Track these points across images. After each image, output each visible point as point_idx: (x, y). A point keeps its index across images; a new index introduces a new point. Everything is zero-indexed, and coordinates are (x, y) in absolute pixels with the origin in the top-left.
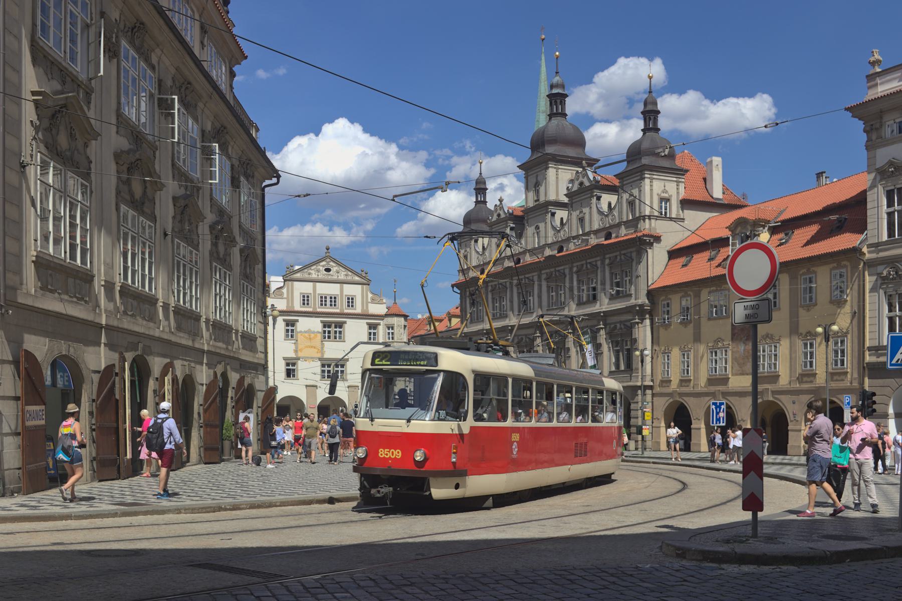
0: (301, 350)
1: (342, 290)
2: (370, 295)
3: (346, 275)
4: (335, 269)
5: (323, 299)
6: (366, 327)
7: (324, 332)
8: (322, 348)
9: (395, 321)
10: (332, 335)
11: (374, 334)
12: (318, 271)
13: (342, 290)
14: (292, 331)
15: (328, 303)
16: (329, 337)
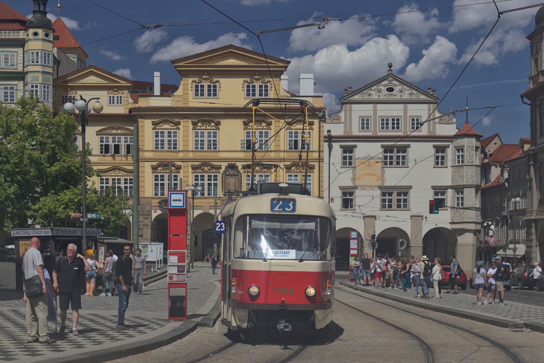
2: (437, 115)
3: (411, 94)
4: (398, 87)
5: (385, 122)
6: (433, 151)
7: (386, 158)
8: (383, 175)
9: (466, 142)
10: (394, 160)
11: (443, 158)
12: (379, 91)
13: (405, 110)
14: (350, 158)
15: (390, 126)
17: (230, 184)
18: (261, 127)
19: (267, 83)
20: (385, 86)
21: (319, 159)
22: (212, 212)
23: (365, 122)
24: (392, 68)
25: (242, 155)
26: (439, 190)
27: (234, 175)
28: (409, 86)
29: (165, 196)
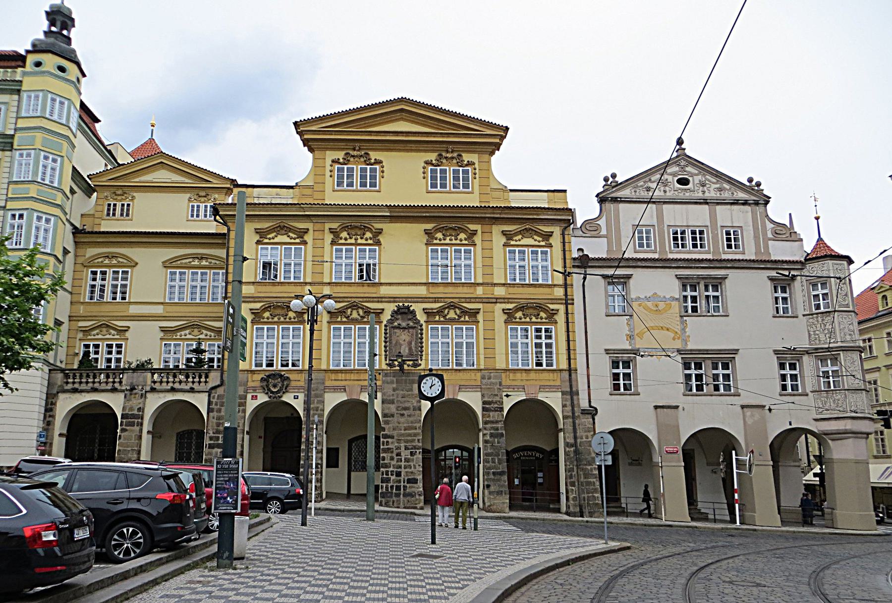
0: (640, 335)
1: (713, 217)
3: (720, 190)
6: (769, 285)
8: (684, 330)
10: (701, 304)
13: (713, 217)
15: (689, 242)
16: (695, 309)
17: (401, 345)
18: (458, 242)
19: (467, 165)
20: (674, 175)
21: (566, 300)
22: (365, 397)
23: (644, 235)
24: (683, 146)
25: (422, 291)
26: (788, 359)
27: (409, 328)
28: (717, 176)
29: (275, 368)
